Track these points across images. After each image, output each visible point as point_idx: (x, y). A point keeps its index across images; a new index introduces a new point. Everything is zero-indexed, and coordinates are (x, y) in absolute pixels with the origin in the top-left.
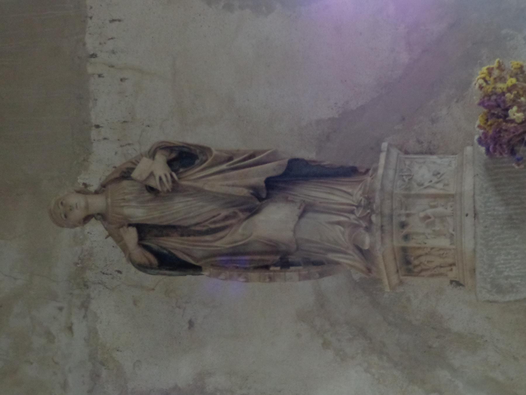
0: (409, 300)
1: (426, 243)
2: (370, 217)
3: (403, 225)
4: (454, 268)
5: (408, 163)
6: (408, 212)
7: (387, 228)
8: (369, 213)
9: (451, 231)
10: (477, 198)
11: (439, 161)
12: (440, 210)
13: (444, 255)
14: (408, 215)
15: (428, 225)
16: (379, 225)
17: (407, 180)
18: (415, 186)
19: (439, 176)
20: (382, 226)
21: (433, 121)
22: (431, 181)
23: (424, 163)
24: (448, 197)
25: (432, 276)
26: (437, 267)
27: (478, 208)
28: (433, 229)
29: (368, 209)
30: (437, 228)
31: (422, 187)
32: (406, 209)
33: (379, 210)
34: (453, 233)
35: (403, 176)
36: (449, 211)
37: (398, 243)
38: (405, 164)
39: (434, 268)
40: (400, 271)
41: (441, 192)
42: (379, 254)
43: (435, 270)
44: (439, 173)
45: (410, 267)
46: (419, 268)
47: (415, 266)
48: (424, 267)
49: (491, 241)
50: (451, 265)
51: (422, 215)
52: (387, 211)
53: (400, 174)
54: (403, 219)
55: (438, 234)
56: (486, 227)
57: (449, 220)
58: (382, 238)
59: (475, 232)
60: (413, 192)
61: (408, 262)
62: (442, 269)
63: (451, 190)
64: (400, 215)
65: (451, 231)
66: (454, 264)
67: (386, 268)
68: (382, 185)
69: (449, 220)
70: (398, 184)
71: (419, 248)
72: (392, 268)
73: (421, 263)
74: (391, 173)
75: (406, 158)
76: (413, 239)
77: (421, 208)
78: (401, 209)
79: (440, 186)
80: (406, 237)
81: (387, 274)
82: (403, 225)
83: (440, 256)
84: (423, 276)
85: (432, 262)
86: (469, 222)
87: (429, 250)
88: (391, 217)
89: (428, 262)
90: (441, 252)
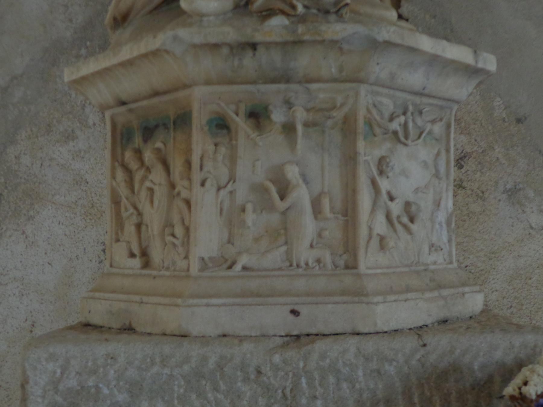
0: (70, 137)
1: (203, 184)
2: (283, 13)
3: (257, 116)
4: (137, 262)
5: (438, 129)
6: (300, 128)
7: (249, 63)
8: (294, 7)
9: (244, 260)
10: (352, 342)
11: (441, 217)
12: (309, 226)
13: (169, 238)
14: (289, 129)
15: (260, 190)
16: (258, 38)
17: (395, 125)
18: (378, 153)
19: (405, 220)
20: (254, 46)
21: (513, 193)
22: (392, 199)
23: (437, 175)
24: (349, 248)
25: (116, 202)
26: (140, 214)
27: (320, 345)
28: (249, 207)
29: (305, 7)
30: (250, 217)
31: (375, 172)
32: (306, 125)
33: (306, 37)
34: (238, 267)
35: (404, 114)
36: (304, 254)
37: (203, 101)
38: (433, 122)
39: (136, 208)
40: (123, 109)
41: (363, 232)
42: (160, 40)
43: (132, 210)
44: (412, 220)
45: (138, 140)
46: (134, 165)
47: (138, 152)
48: (138, 177)
49: (216, 389)
50: (144, 254)
51: (292, 173)
52: (304, 61)
53: (411, 108)
54: (278, 116)
55: (233, 219)
56: (259, 372)
57: (277, 256)
58: (216, 46)
59: (241, 339)
60: (361, 145)
61: (148, 133)
62: (133, 228)
63: (369, 260)
64: (289, 104)
65: (244, 260)
66: (146, 265)
67: (123, 64)
68: (388, 44)
69: (277, 256)
70: (385, 100)
71: (188, 164)
72: (131, 85)
73: (148, 170)
74: (415, 79)
75: (448, 126)
76: (216, 145)
77: (312, 167)
78: (308, 110)
79: (380, 226)
80: (221, 125)
81: (107, 70)
82: (257, 116)
83: (168, 225)
84: (114, 177)
85: (152, 202)
86: (274, 318)
87: (184, 194)
88: (285, 78)
89: (151, 190)
90: (179, 231)
